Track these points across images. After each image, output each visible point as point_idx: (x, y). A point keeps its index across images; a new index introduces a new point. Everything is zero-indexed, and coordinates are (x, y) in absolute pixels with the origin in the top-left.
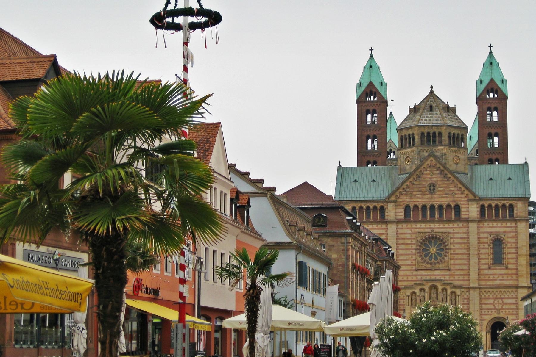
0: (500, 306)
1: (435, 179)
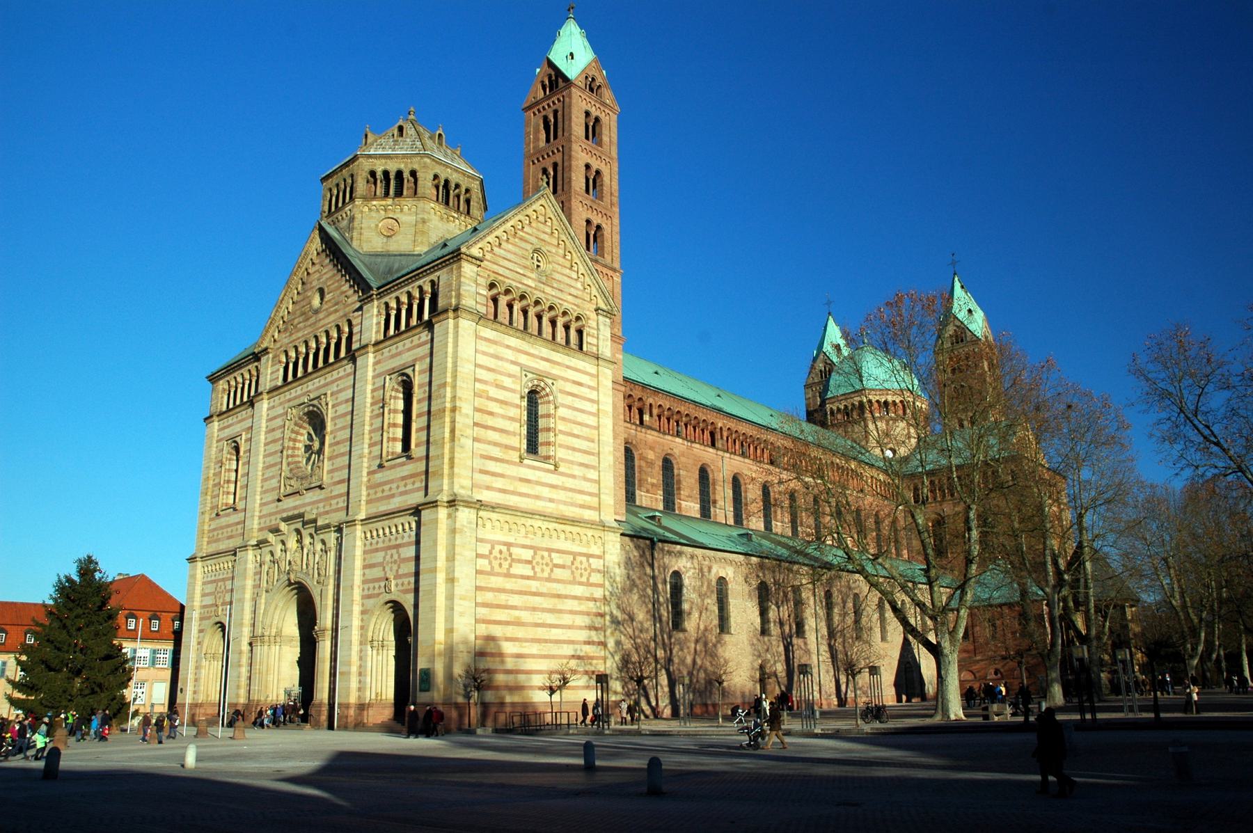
0: (395, 567)
1: (324, 278)
